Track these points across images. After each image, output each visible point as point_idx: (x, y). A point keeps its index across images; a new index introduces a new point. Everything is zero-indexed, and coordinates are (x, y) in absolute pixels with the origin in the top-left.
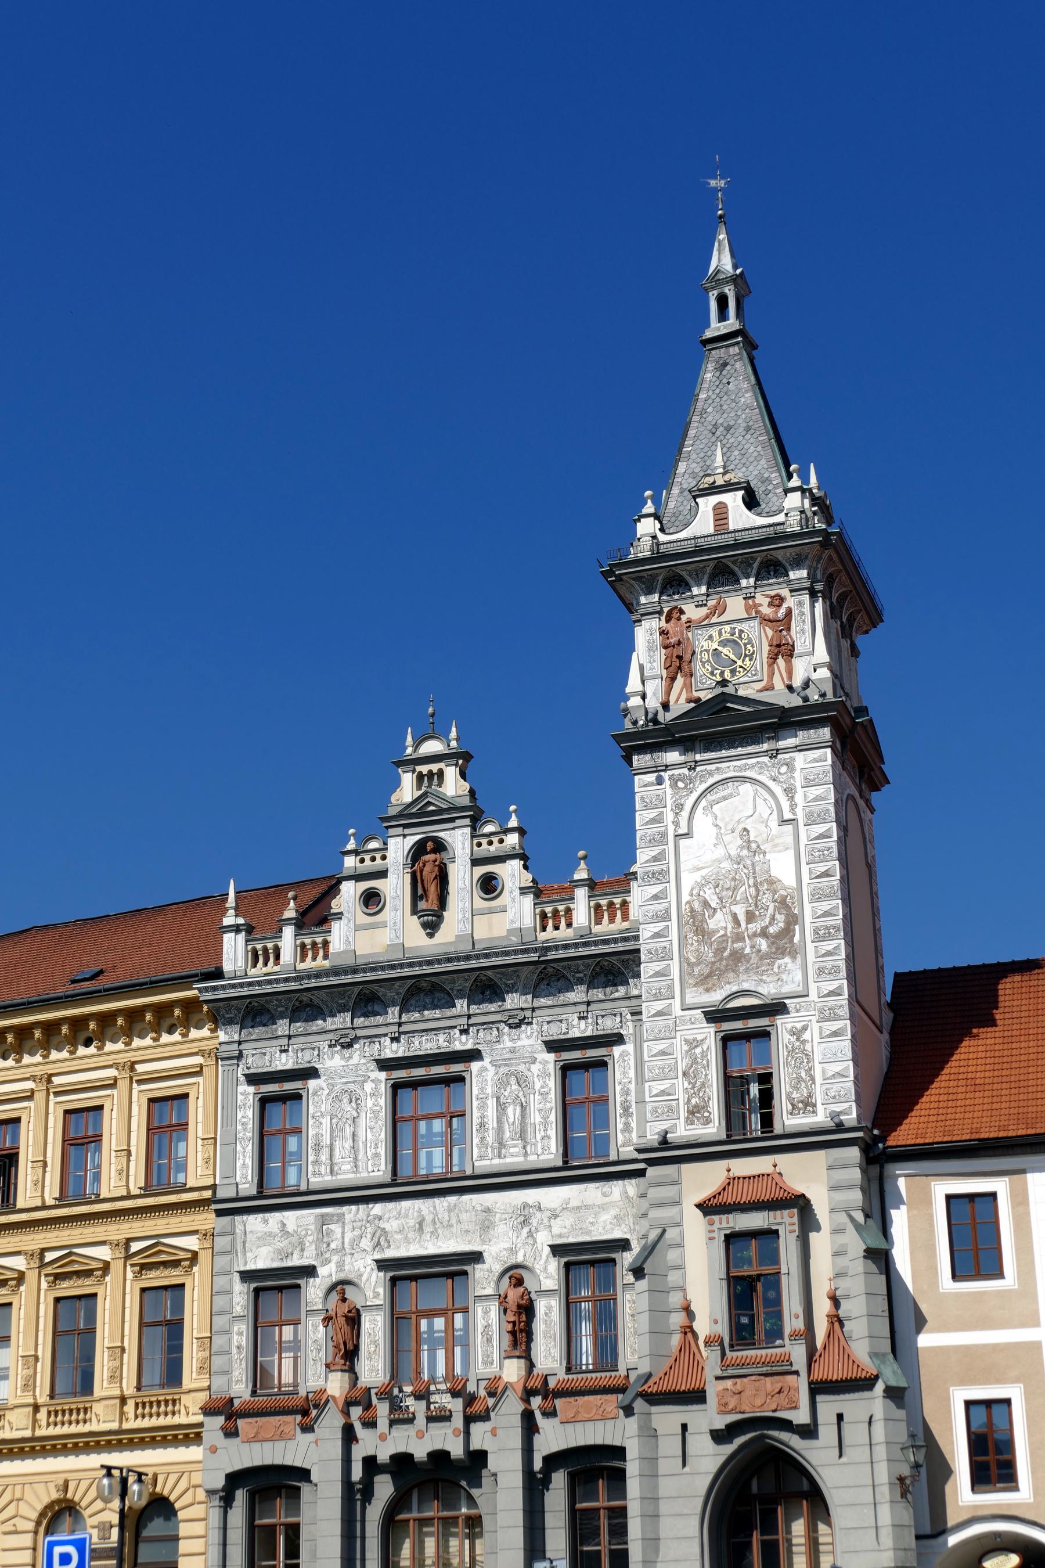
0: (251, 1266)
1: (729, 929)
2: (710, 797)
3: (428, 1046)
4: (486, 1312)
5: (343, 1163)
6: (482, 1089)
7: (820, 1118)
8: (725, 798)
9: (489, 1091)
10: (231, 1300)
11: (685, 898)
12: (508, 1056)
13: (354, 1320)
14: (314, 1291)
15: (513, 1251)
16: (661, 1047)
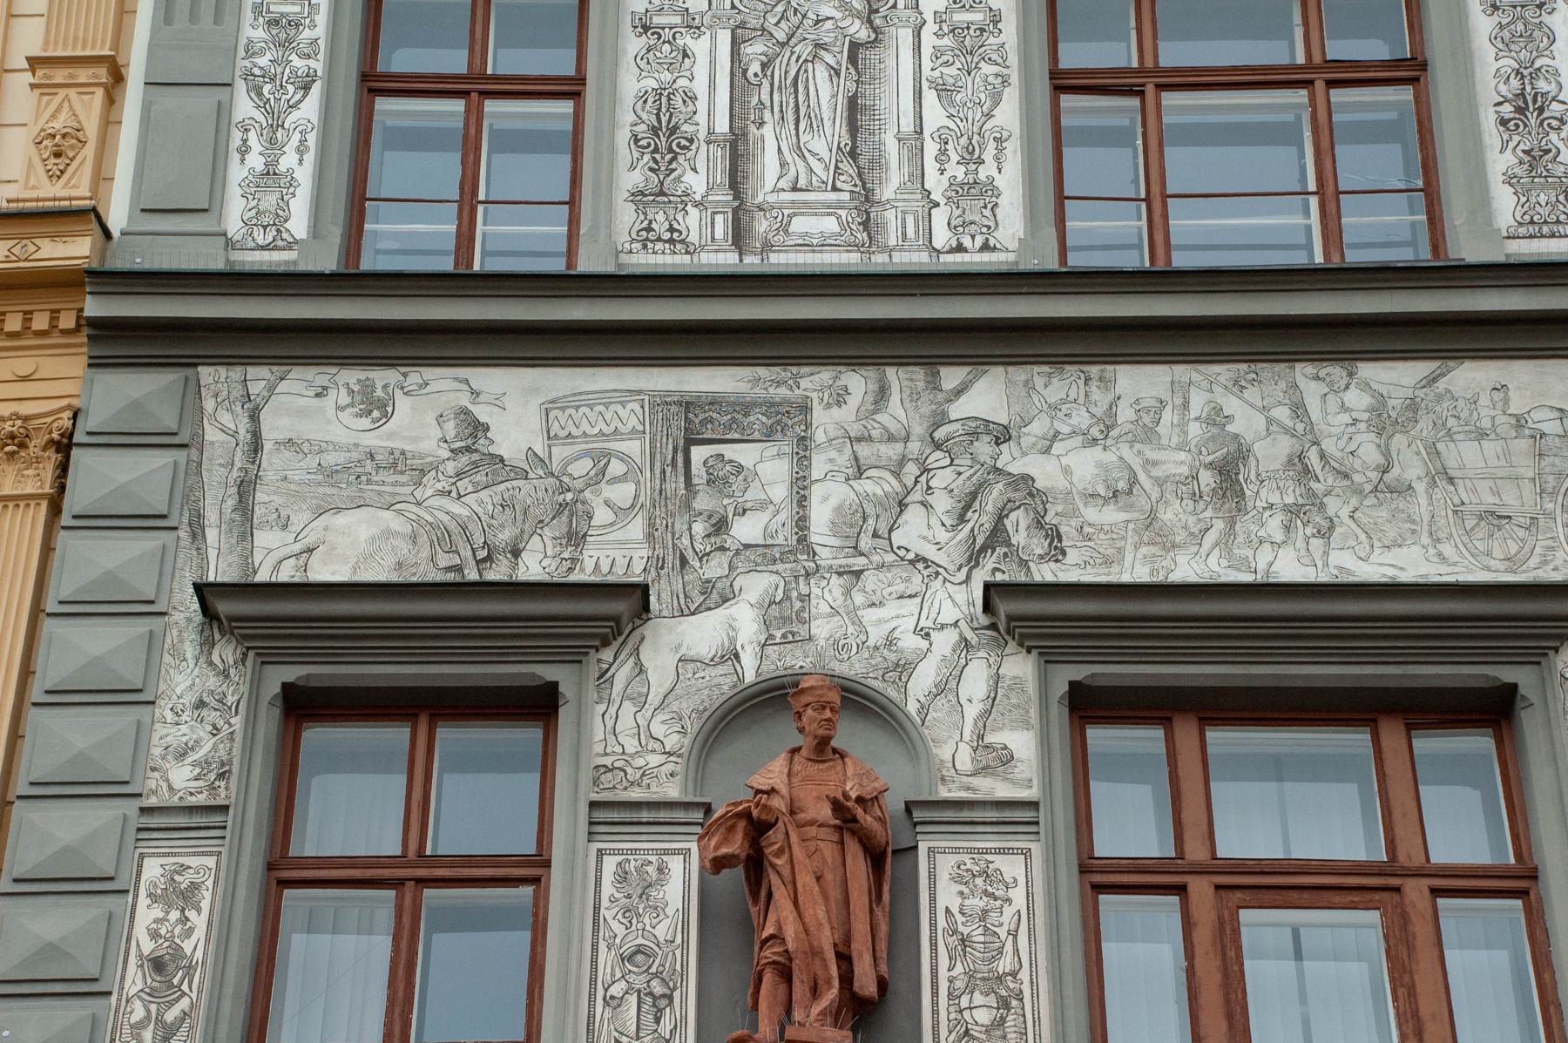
14: (637, 720)
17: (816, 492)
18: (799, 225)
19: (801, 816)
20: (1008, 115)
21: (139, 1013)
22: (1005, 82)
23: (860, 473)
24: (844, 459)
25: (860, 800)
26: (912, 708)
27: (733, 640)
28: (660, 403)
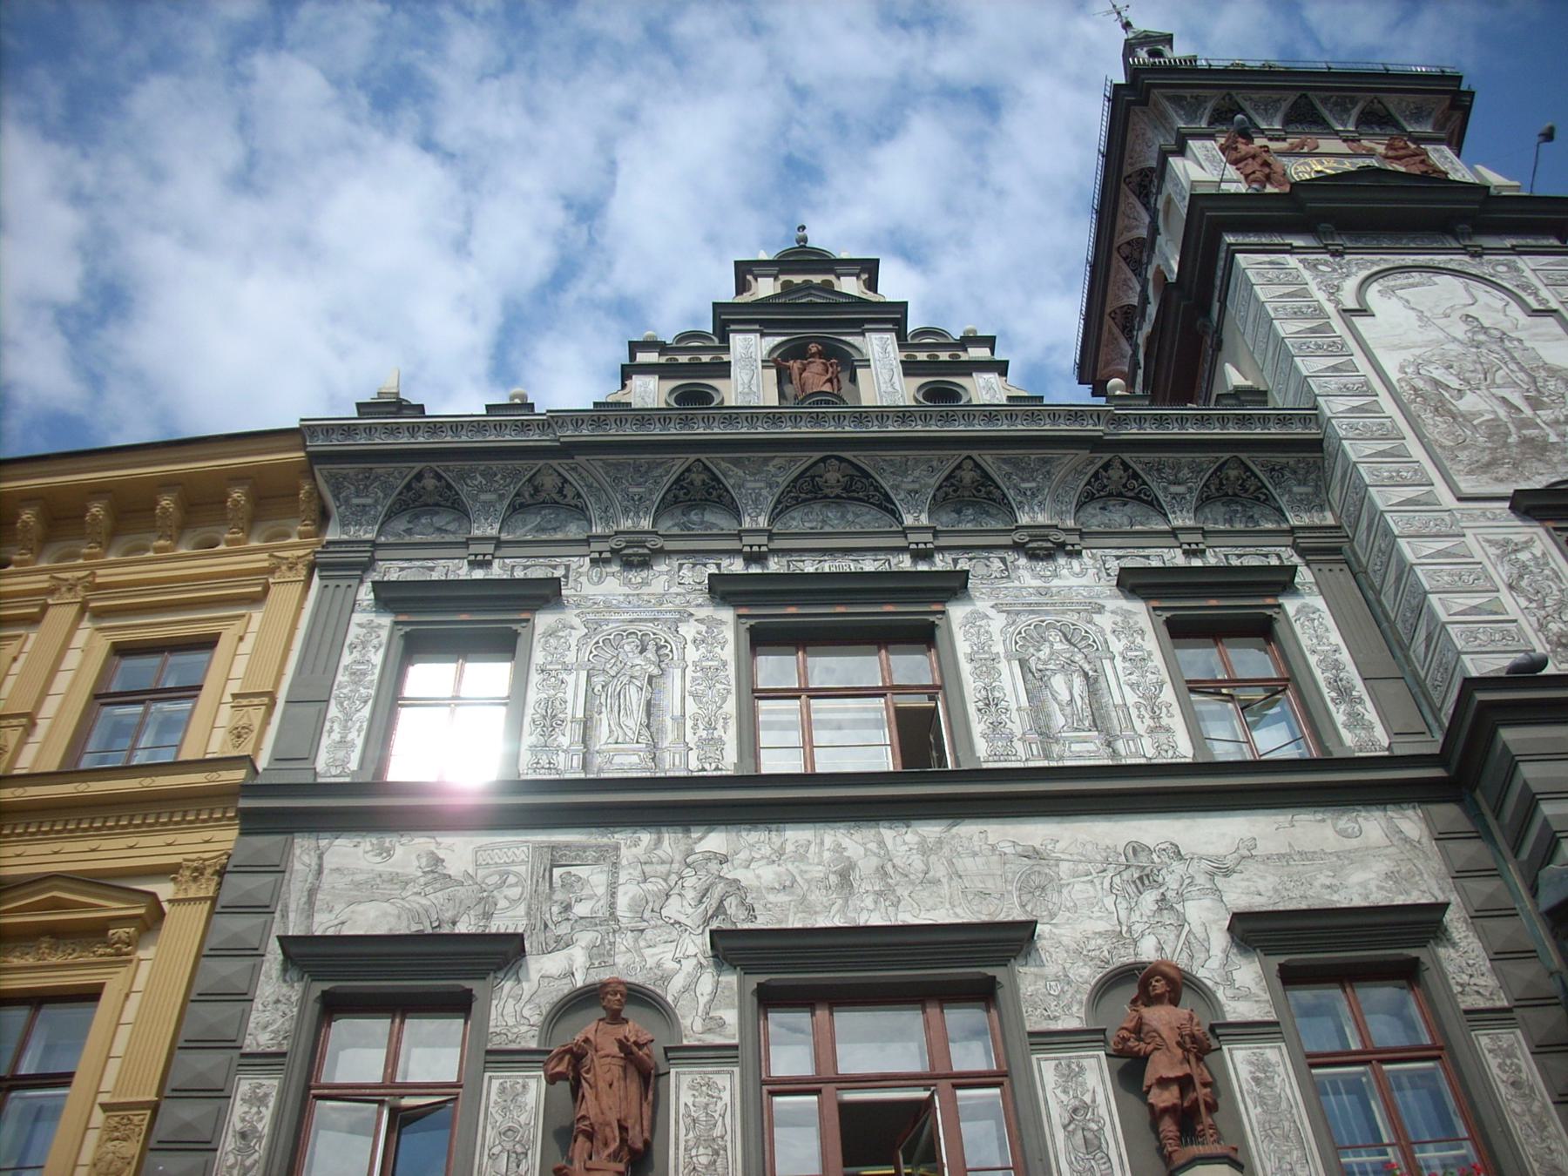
5: (618, 752)
9: (999, 648)
10: (244, 1018)
11: (1394, 376)
12: (1034, 599)
14: (516, 1009)
15: (1120, 937)
17: (621, 890)
18: (617, 760)
19: (602, 1053)
20: (730, 706)
21: (231, 1160)
22: (729, 692)
23: (645, 881)
24: (637, 873)
25: (635, 1043)
26: (670, 999)
27: (571, 966)
28: (538, 848)
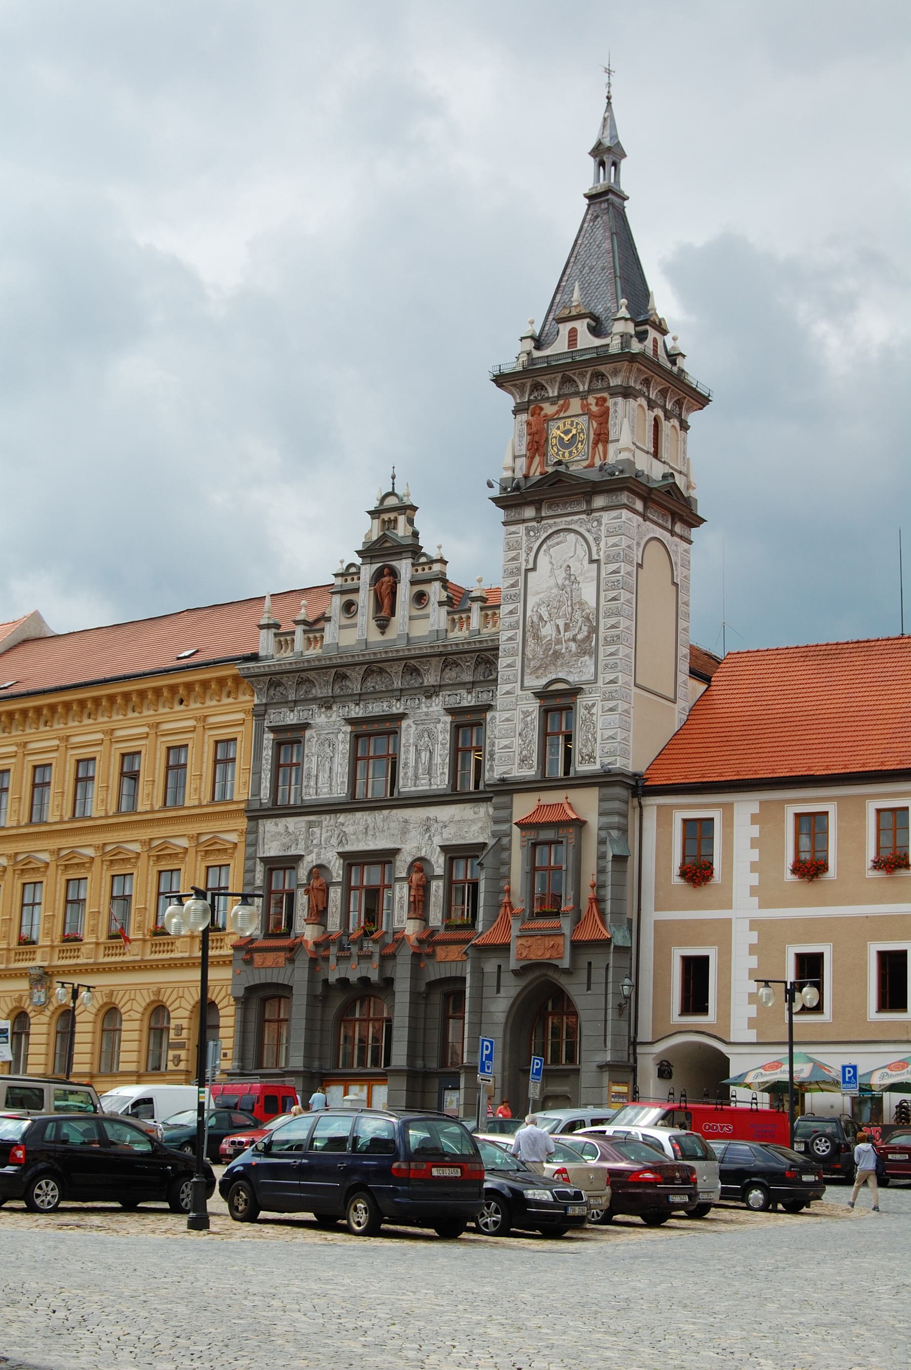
0: (267, 854)
1: (554, 636)
2: (549, 543)
3: (377, 710)
4: (401, 889)
5: (324, 787)
6: (408, 740)
7: (596, 767)
8: (558, 544)
9: (411, 741)
11: (529, 613)
12: (424, 718)
13: (325, 890)
14: (302, 873)
15: (419, 849)
16: (507, 716)
